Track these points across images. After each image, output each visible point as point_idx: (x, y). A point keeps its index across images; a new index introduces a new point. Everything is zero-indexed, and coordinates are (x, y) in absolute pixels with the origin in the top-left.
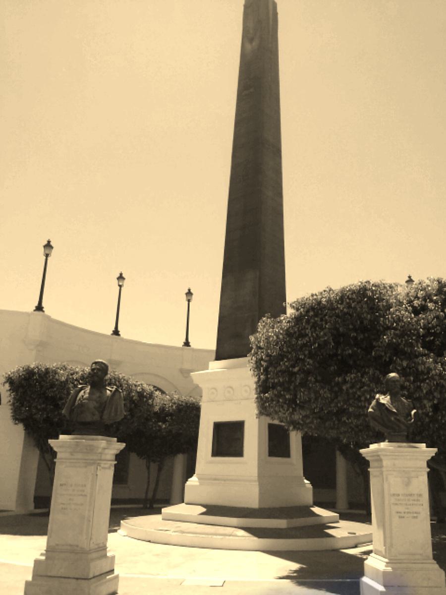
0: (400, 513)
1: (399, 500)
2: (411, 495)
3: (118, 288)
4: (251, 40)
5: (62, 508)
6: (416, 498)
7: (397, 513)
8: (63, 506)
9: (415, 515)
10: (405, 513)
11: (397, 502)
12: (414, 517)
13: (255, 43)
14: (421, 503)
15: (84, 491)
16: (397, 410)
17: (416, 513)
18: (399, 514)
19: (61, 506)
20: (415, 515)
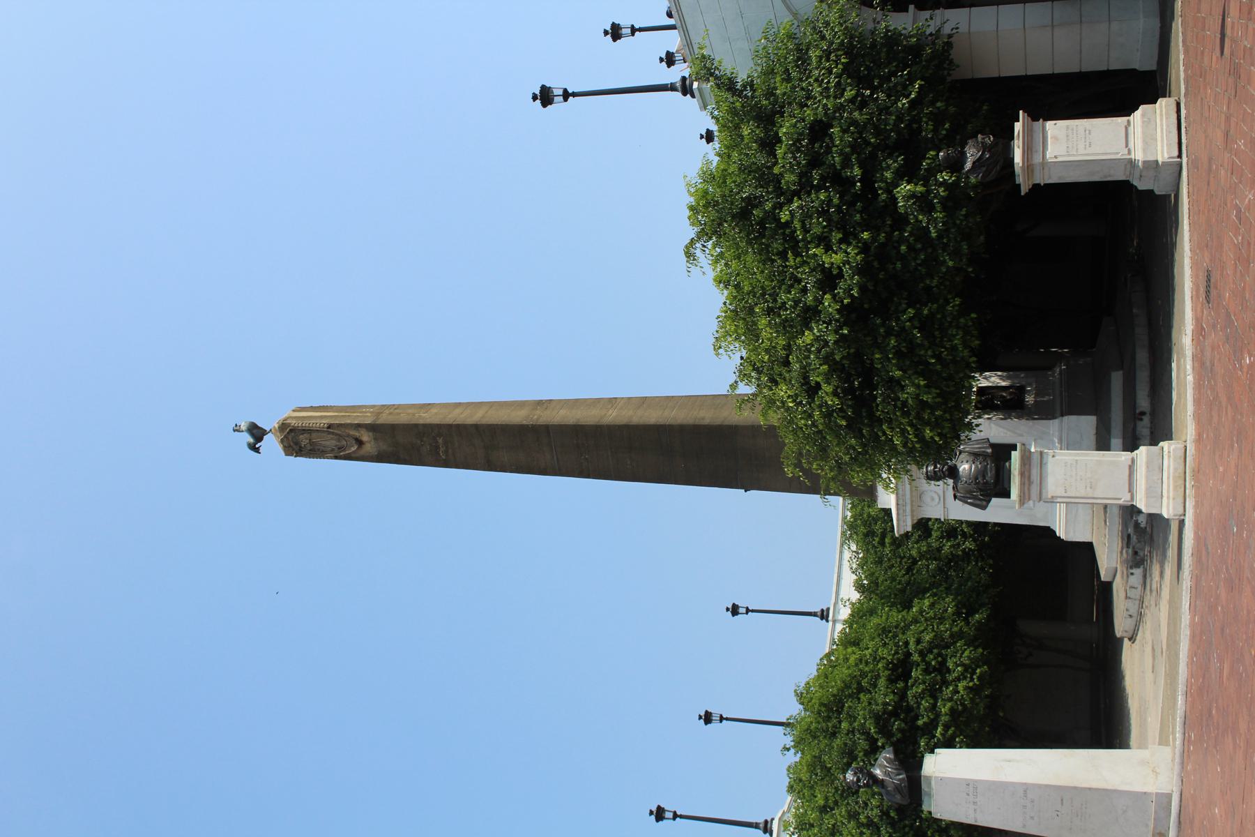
0: (1085, 145)
1: (1073, 147)
2: (1067, 136)
3: (724, 721)
4: (360, 443)
5: (1091, 488)
6: (1070, 131)
7: (1085, 148)
8: (1089, 486)
9: (1087, 132)
10: (1085, 142)
11: (1075, 149)
12: (1090, 134)
13: (366, 436)
14: (1075, 127)
15: (1071, 464)
16: (979, 152)
17: (1085, 131)
18: (1087, 146)
19: (1088, 489)
20: (1087, 132)
